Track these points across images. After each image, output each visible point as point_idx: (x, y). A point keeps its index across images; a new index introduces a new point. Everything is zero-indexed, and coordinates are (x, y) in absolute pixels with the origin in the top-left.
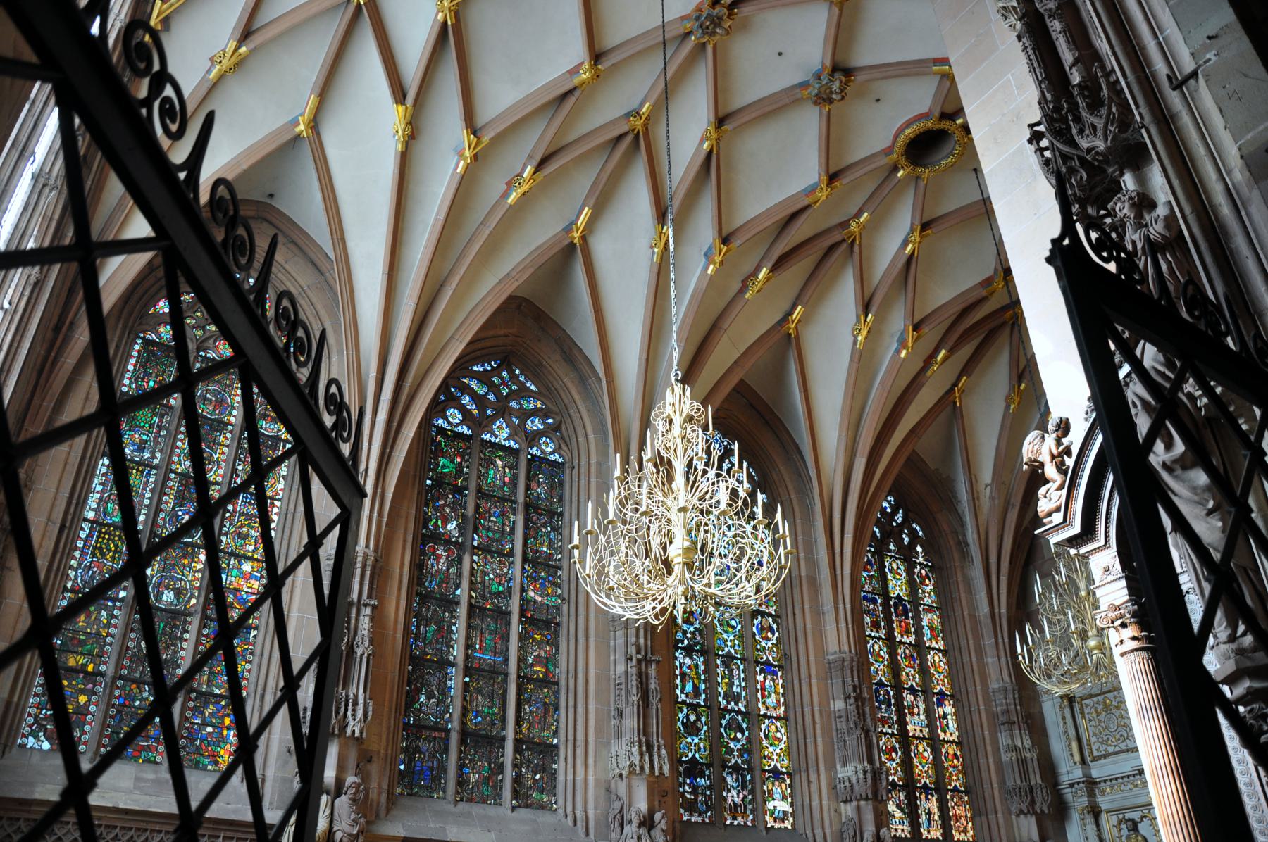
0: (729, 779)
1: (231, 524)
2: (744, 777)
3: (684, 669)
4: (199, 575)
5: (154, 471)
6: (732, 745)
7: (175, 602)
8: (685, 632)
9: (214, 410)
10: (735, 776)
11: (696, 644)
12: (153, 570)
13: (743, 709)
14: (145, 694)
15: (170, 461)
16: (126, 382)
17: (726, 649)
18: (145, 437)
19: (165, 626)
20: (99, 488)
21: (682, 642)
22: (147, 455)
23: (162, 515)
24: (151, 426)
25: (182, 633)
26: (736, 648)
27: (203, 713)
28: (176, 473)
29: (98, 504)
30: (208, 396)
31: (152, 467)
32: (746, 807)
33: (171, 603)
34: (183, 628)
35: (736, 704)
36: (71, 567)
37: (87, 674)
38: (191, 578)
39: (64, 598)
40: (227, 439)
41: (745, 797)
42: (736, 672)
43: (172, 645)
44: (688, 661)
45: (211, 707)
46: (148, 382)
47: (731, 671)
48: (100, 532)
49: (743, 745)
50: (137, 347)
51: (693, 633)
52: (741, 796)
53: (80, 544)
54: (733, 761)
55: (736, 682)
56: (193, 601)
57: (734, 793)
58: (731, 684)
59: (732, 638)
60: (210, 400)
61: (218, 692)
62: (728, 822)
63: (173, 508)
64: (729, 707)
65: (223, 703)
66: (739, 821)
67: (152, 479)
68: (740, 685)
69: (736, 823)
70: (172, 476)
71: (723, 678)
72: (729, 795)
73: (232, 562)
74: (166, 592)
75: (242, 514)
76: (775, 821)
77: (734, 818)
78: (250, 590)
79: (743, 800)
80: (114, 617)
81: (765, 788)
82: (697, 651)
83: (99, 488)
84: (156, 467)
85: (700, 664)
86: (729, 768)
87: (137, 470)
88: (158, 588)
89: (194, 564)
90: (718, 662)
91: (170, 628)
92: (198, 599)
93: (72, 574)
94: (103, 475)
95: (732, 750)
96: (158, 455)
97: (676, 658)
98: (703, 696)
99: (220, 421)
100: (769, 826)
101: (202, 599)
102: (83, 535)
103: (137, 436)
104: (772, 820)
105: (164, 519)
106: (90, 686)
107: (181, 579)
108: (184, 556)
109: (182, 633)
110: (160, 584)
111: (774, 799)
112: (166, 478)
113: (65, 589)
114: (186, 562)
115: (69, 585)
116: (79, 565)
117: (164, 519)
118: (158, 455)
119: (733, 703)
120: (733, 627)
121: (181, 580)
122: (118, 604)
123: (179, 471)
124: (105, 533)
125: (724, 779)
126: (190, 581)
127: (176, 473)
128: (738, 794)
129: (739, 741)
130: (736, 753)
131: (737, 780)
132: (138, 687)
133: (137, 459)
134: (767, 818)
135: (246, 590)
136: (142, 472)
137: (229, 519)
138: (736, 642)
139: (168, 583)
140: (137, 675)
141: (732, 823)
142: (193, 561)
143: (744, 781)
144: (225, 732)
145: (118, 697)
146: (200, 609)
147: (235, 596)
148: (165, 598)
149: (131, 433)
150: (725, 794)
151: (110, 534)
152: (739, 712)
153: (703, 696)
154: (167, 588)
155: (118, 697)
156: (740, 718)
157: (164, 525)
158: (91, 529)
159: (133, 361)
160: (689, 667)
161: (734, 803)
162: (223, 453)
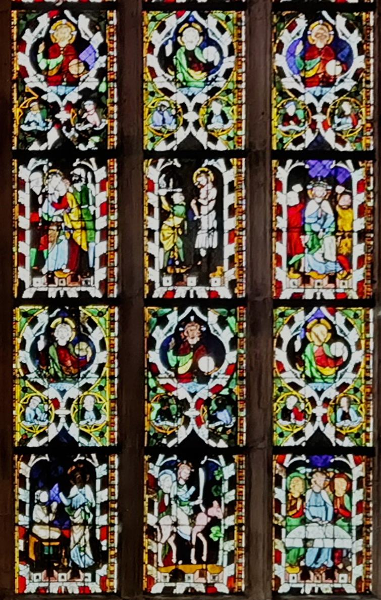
0: (167, 481)
2: (211, 469)
3: (47, 210)
6: (182, 391)
8: (51, 109)
10: (185, 471)
11: (84, 137)
13: (225, 293)
17: (181, 135)
21: (42, 137)
26: (217, 123)
32: (214, 547)
35: (204, 281)
41: (215, 521)
42: (208, 192)
44: (58, 186)
47: (192, 193)
49: (217, 389)
51: (79, 105)
52: (202, 520)
54: (183, 434)
55: (208, 220)
57: (181, 514)
58: (191, 227)
59: (201, 98)
62: (157, 589)
64: (180, 292)
66: (194, 581)
68: (220, 228)
69: (180, 588)
71: (164, 215)
72: (166, 521)
76: (305, 576)
77: (177, 576)
79: (206, 531)
81: (279, 494)
82: (87, 155)
85: (94, 189)
86: (168, 452)
90: (153, 173)
95: (183, 405)
97: (22, 184)
98: (100, 274)
100: (284, 589)
104: (296, 572)
111: (304, 522)
119: (192, 280)
120: (209, 68)
125: (154, 484)
128: (192, 518)
129: (204, 378)
130: (192, 413)
131: (192, 480)
134: (279, 570)
138: (216, 108)
141: (168, 591)
143: (213, 484)
150: (151, 520)
152: (213, 301)
153: (100, 274)
156: (212, 317)
160: (61, 203)
161: (179, 540)
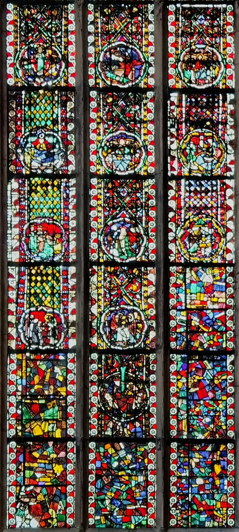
1: (177, 226)
4: (152, 301)
5: (73, 181)
7: (132, 340)
9: (126, 76)
12: (99, 307)
14: (122, 453)
15: (87, 163)
16: (10, 71)
18: (50, 140)
19: (127, 370)
20: (16, 220)
22: (59, 162)
23: (94, 235)
24: (55, 122)
25: (148, 376)
27: (189, 465)
28: (99, 177)
29: (20, 241)
30: (114, 57)
31: (69, 177)
33: (128, 343)
34: (148, 369)
36: (10, 324)
37: (55, 440)
38: (144, 307)
39: (12, 361)
40: (149, 111)
43: (139, 391)
45: (197, 455)
46: (36, 63)
48: (30, 275)
50: (10, 17)
53: (12, 295)
56: (152, 334)
60: (117, 63)
61: (200, 436)
63: (106, 225)
65: (209, 449)
67: (73, 192)
70: (94, 181)
73: (188, 275)
74: (119, 330)
75: (189, 209)
78: (216, 306)
80: (68, 371)
83: (16, 220)
84: (73, 175)
87: (53, 186)
88: (110, 326)
89: (144, 289)
91: (134, 372)
92: (157, 330)
93: (12, 331)
94: (16, 203)
96: (71, 158)
99: (136, 89)
101: (161, 330)
102: (13, 283)
103: (41, 141)
105: (97, 241)
106: (62, 454)
107: (133, 311)
108: (131, 282)
109: (148, 376)
110: (110, 322)
112: (88, 187)
113: (10, 351)
114: (134, 287)
115: (13, 344)
116: (18, 319)
117: (97, 241)
118: (71, 158)
121: (133, 311)
122: (70, 356)
123: (101, 172)
124: (37, 274)
126: (144, 311)
127: (99, 177)
132: (113, 447)
133: (49, 171)
135: (211, 306)
136: (59, 187)
137: (174, 219)
139: (120, 320)
140: (109, 433)
142: (141, 285)
144: (218, 482)
145: (94, 462)
146: (161, 341)
147: (200, 317)
148: (119, 337)
149: (33, 139)
151: (42, 275)
154: (120, 325)
155: (94, 462)
157: (100, 246)
158: (21, 274)
159: (10, 39)
162: (149, 132)
